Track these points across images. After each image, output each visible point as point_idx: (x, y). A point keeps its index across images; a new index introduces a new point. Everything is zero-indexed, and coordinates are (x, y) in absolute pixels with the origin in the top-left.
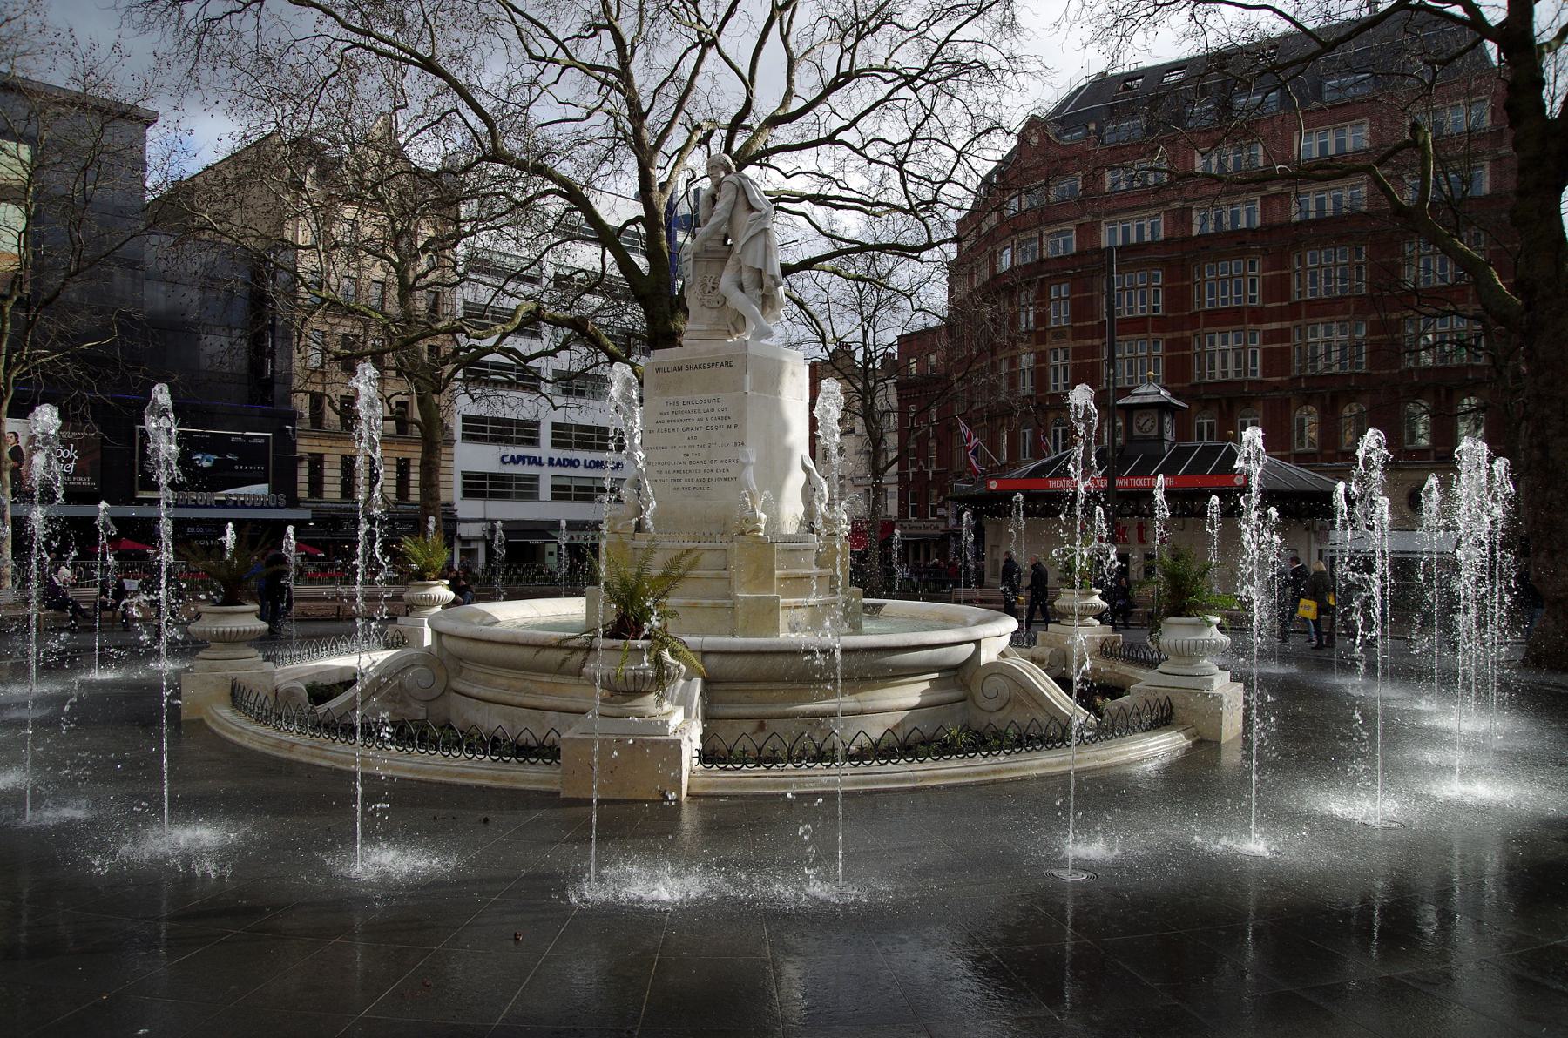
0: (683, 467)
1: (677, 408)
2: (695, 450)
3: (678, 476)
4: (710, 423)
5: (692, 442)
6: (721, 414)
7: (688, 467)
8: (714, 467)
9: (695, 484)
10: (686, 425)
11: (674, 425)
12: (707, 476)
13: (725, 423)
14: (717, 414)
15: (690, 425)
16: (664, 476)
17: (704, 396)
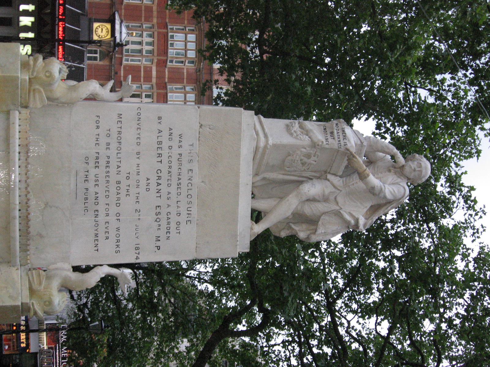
0: (113, 170)
1: (185, 159)
2: (133, 191)
3: (102, 162)
4: (164, 211)
5: (143, 183)
6: (173, 225)
7: (113, 178)
8: (112, 219)
9: (92, 190)
10: (164, 175)
11: (165, 158)
12: (101, 208)
13: (162, 233)
14: (174, 219)
15: (163, 181)
16: (103, 141)
17: (195, 200)
